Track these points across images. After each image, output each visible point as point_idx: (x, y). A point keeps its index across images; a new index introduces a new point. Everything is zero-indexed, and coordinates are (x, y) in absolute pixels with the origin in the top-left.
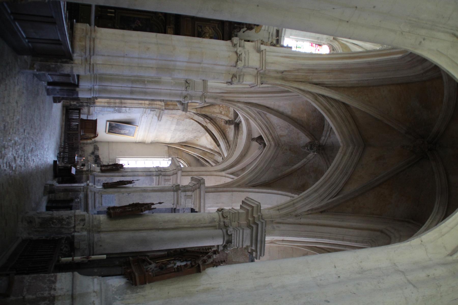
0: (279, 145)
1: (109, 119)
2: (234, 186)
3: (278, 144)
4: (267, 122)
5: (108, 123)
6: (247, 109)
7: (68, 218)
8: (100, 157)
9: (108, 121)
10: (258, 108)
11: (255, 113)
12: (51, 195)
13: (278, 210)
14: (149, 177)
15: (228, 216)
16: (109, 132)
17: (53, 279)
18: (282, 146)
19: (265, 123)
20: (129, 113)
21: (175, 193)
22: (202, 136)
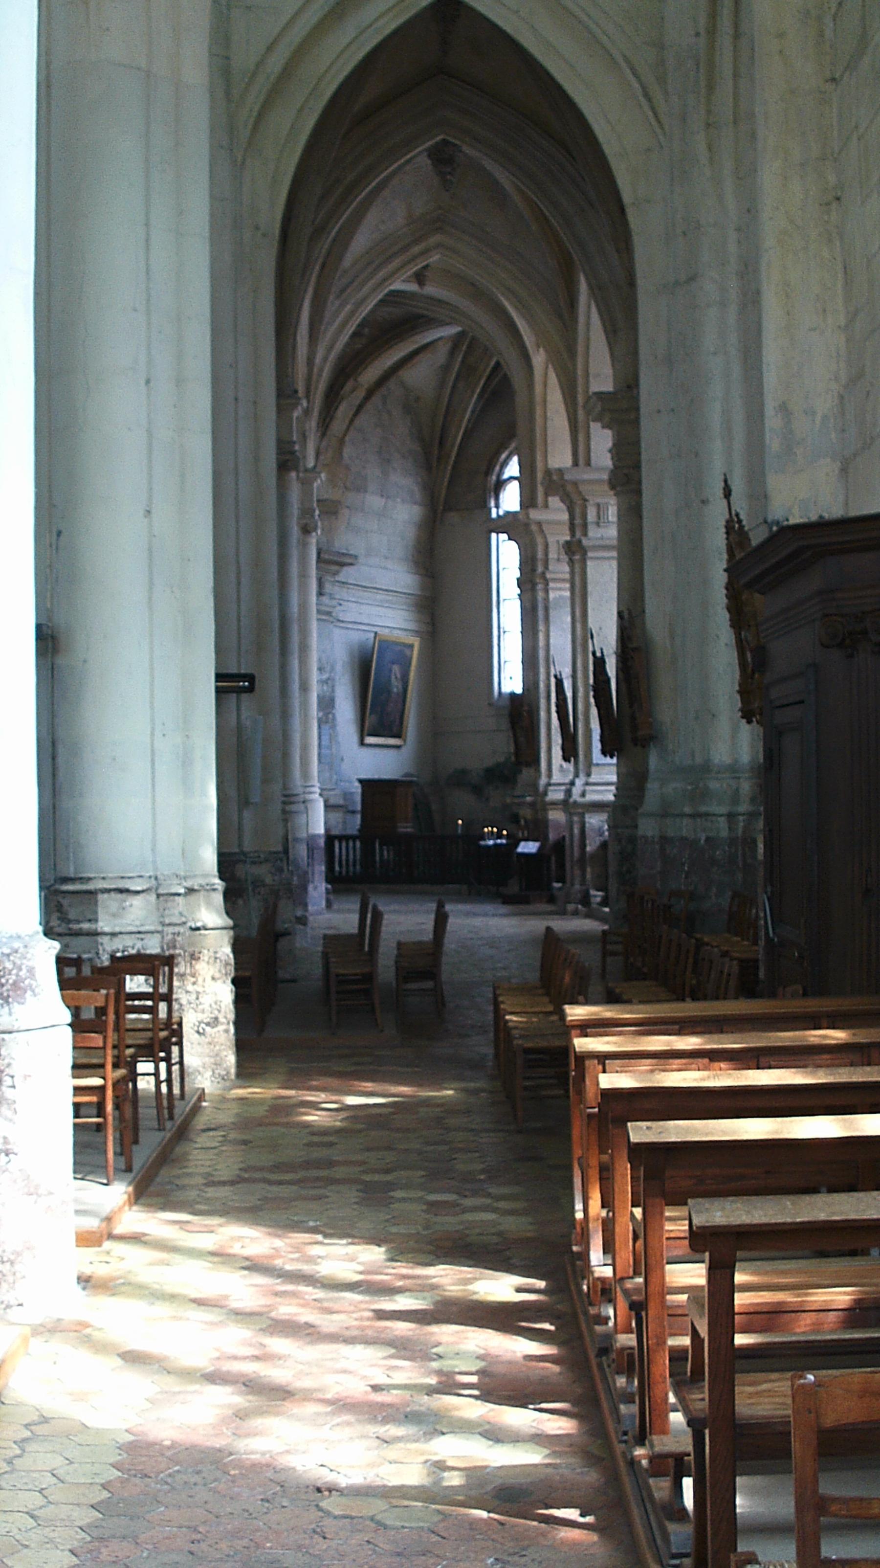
1: (355, 738)
3: (437, 222)
4: (369, 264)
5: (370, 740)
7: (620, 841)
8: (489, 762)
9: (362, 743)
11: (342, 306)
12: (593, 900)
13: (615, 332)
14: (552, 613)
15: (625, 471)
16: (398, 736)
17: (643, 840)
18: (440, 208)
19: (370, 270)
20: (333, 669)
21: (590, 554)
22: (402, 384)
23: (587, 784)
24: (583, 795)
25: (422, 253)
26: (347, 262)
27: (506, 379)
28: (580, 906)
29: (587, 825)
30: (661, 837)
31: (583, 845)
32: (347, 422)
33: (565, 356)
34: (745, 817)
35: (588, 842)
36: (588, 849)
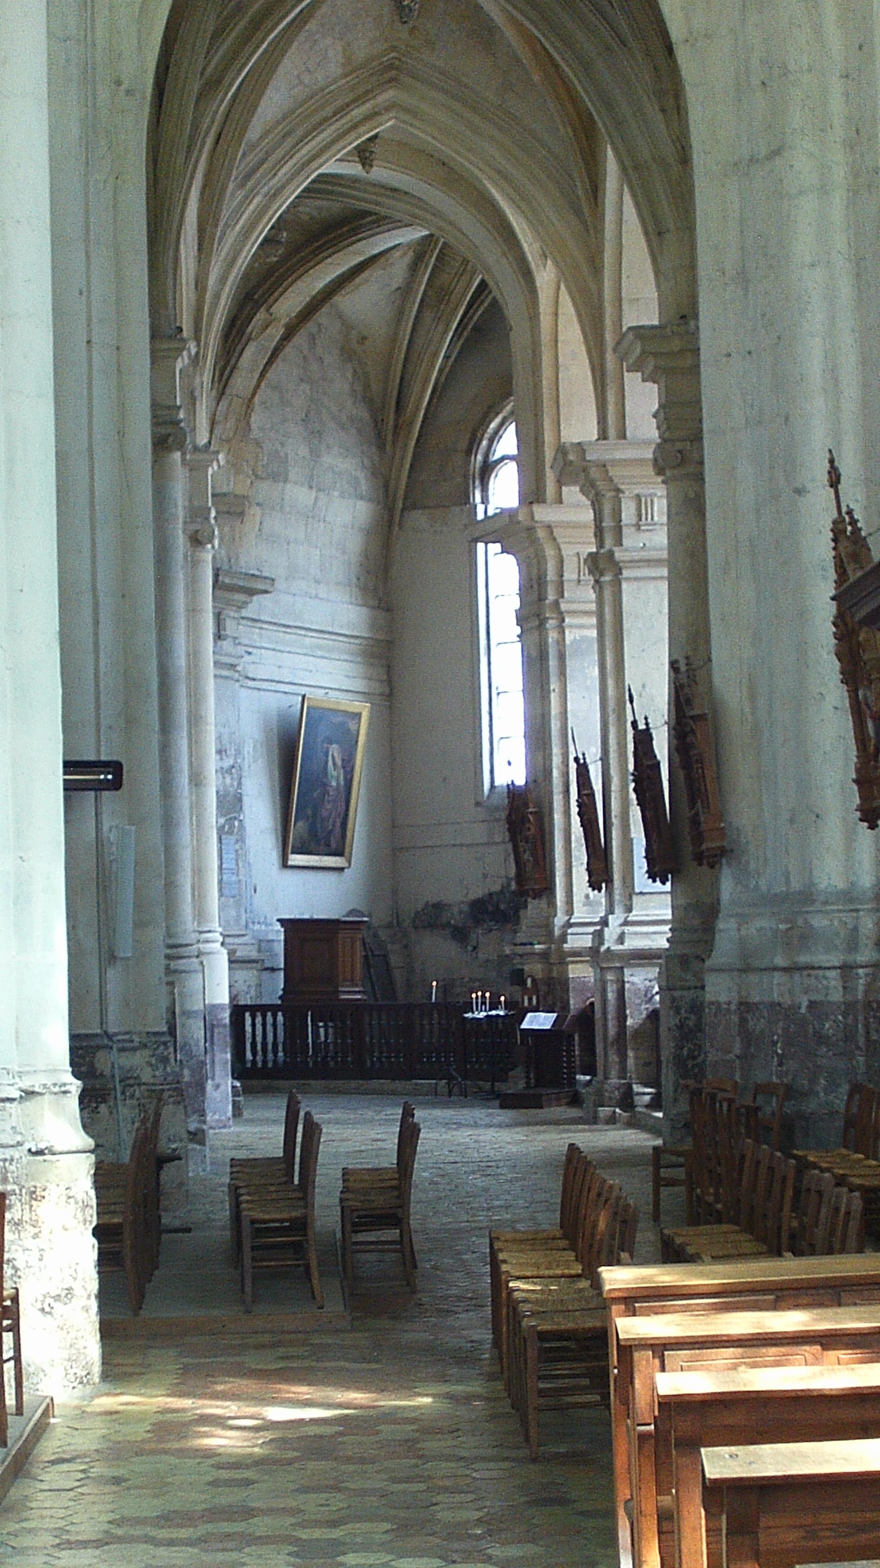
0: (391, 67)
2: (594, 288)
3: (389, 71)
6: (231, 238)
10: (224, 188)
18: (394, 48)
23: (626, 923)
24: (621, 939)
25: (368, 118)
26: (253, 133)
27: (495, 307)
28: (618, 1110)
29: (627, 986)
30: (741, 1003)
31: (622, 1017)
32: (256, 376)
33: (585, 268)
34: (867, 970)
35: (628, 1012)
36: (629, 1022)
